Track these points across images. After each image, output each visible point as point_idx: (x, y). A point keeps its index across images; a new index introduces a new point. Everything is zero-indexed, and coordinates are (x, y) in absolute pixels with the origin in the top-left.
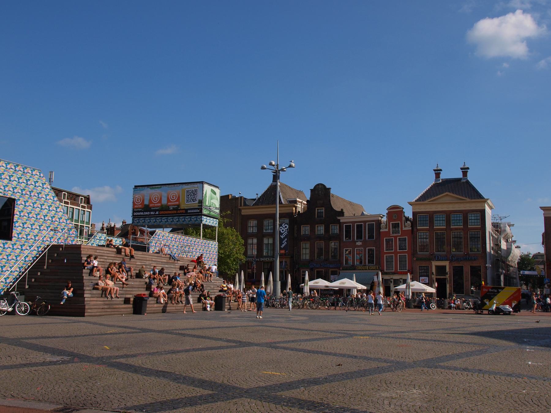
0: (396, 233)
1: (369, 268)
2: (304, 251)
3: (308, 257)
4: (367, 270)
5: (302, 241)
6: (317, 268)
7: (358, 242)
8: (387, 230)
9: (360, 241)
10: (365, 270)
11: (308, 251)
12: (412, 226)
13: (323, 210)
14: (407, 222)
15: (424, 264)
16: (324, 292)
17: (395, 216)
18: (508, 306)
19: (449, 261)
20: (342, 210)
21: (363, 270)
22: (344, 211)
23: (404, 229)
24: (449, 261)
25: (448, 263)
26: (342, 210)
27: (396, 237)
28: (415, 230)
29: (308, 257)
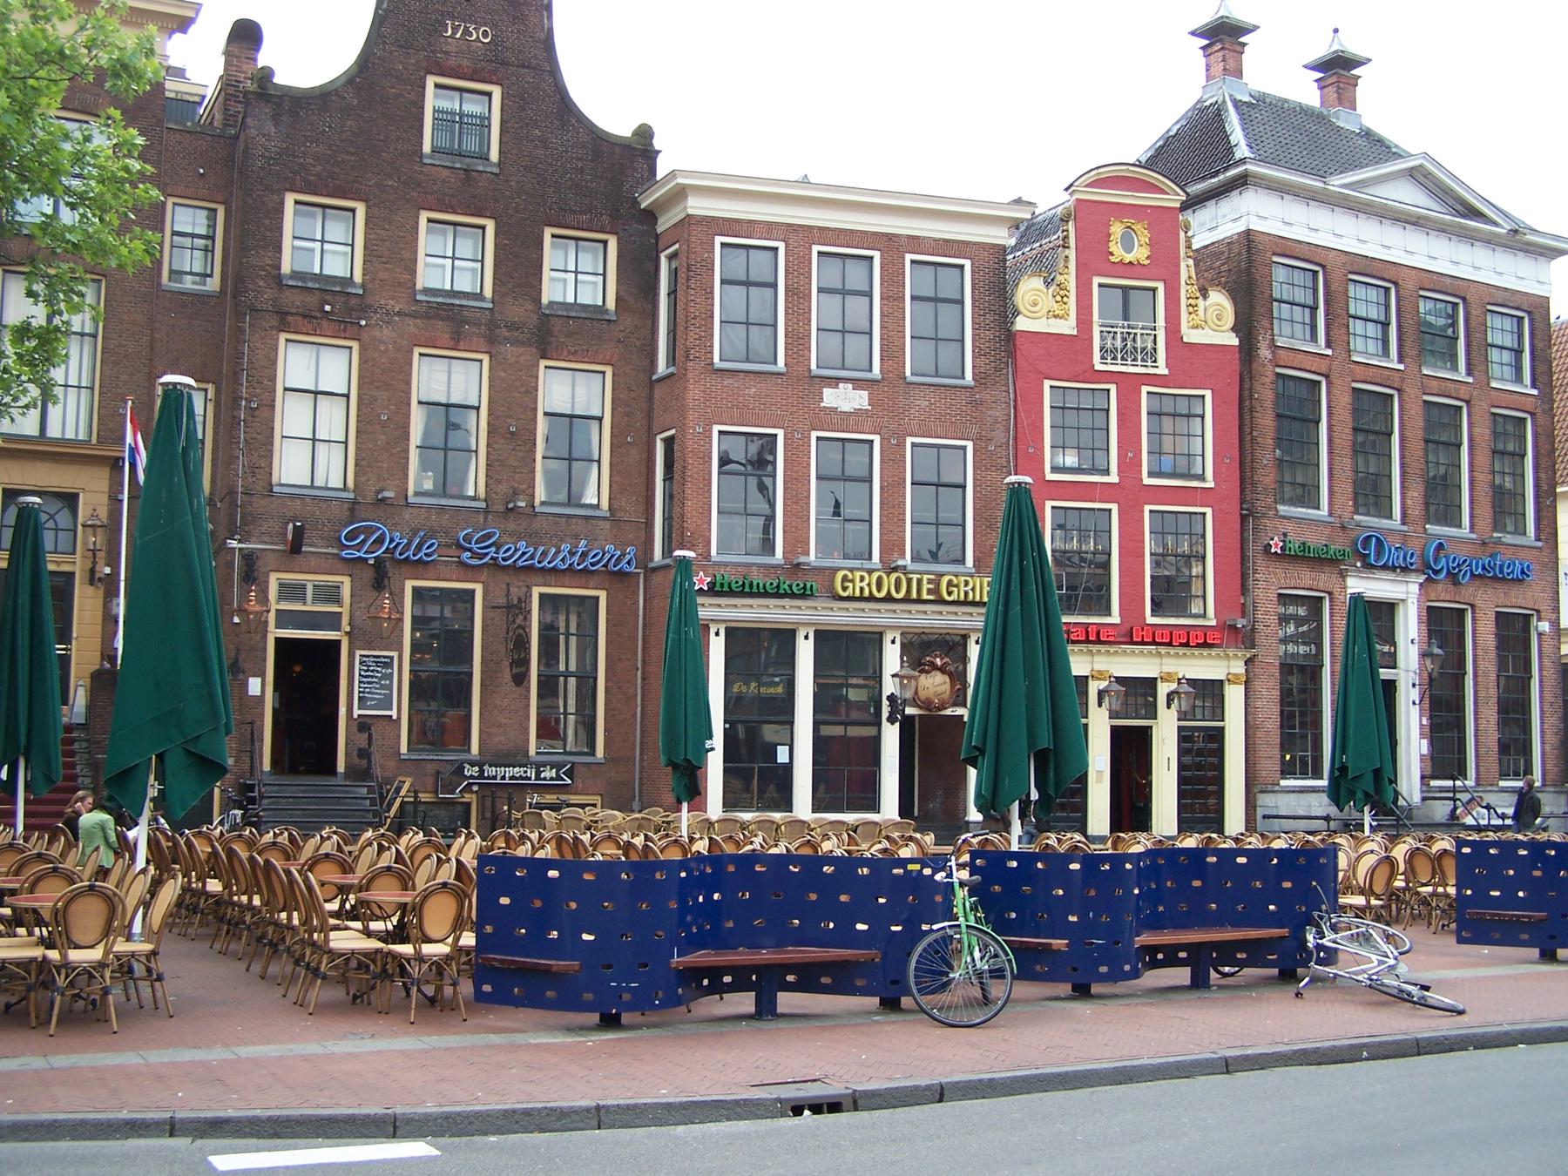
0: (1129, 354)
1: (935, 591)
2: (292, 417)
3: (334, 471)
4: (919, 601)
5: (284, 327)
6: (420, 567)
7: (834, 382)
8: (1068, 327)
9: (858, 384)
10: (907, 600)
11: (334, 420)
12: (1245, 326)
13: (490, 104)
14: (1205, 297)
15: (1304, 581)
16: (490, 771)
17: (1128, 246)
18: (156, 794)
19: (1422, 578)
20: (645, 133)
21: (889, 599)
22: (657, 143)
23: (1191, 336)
24: (1422, 578)
25: (1415, 588)
26: (645, 133)
27: (1129, 385)
28: (1264, 352)
29: (334, 471)
